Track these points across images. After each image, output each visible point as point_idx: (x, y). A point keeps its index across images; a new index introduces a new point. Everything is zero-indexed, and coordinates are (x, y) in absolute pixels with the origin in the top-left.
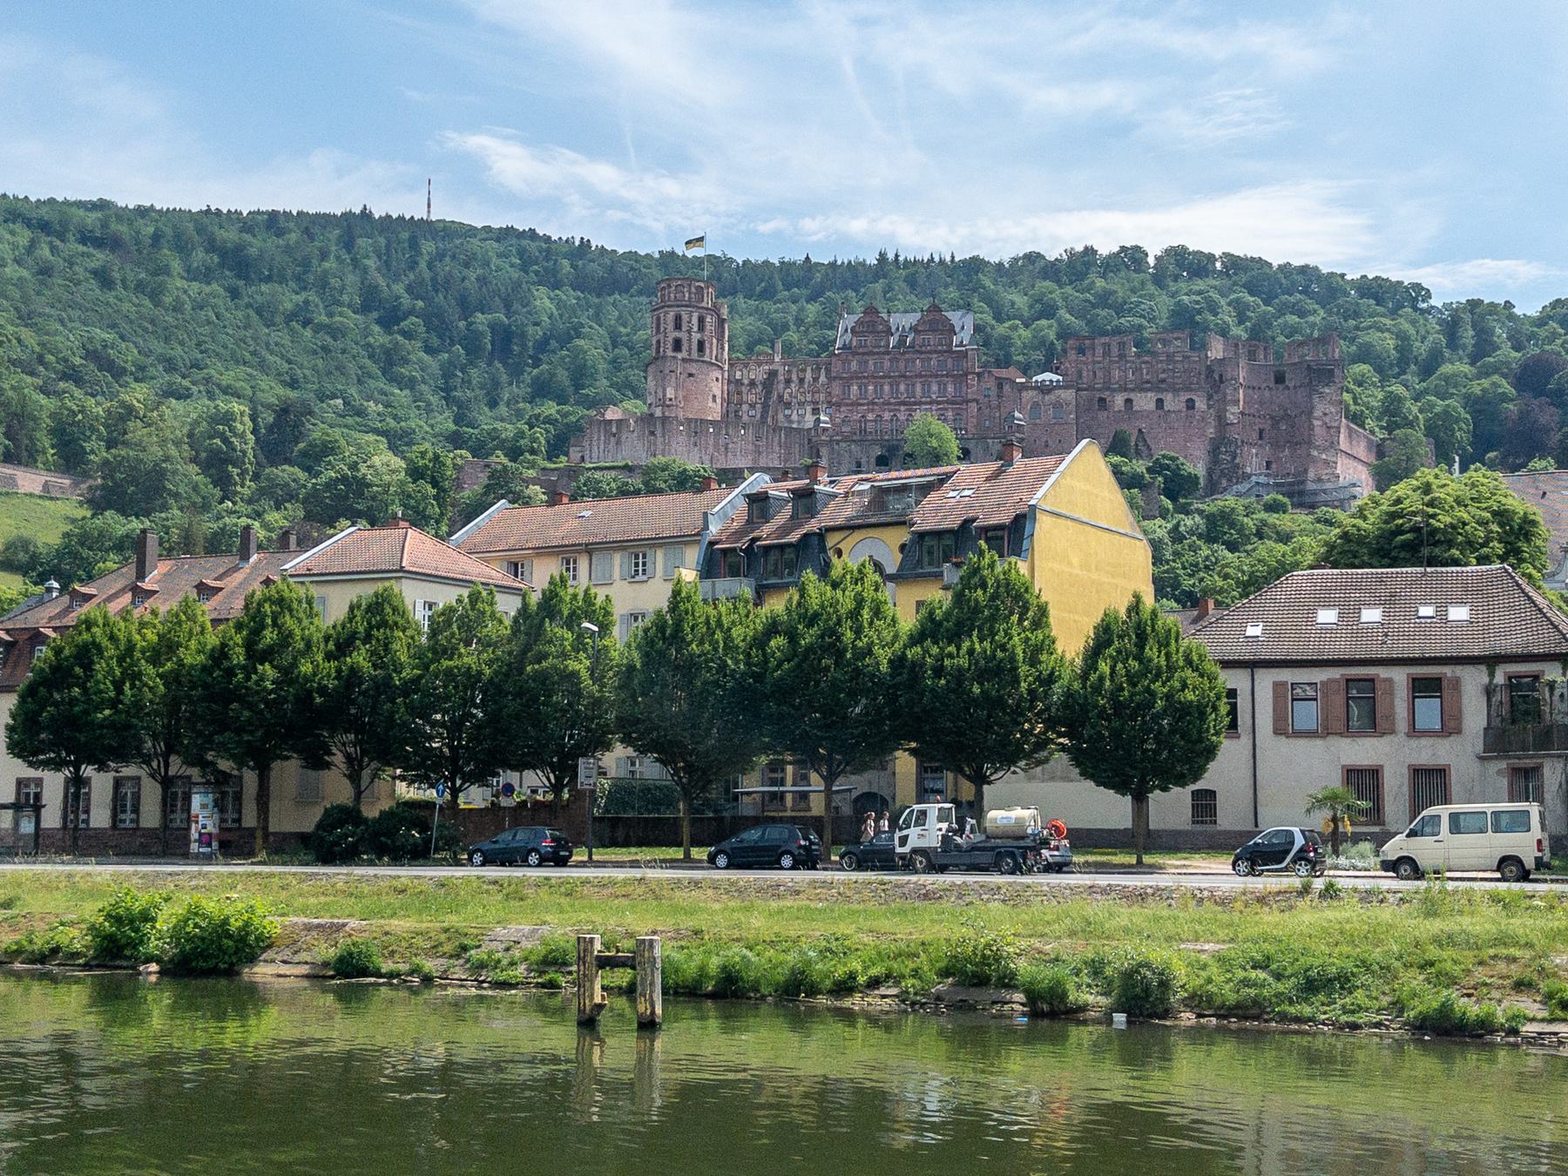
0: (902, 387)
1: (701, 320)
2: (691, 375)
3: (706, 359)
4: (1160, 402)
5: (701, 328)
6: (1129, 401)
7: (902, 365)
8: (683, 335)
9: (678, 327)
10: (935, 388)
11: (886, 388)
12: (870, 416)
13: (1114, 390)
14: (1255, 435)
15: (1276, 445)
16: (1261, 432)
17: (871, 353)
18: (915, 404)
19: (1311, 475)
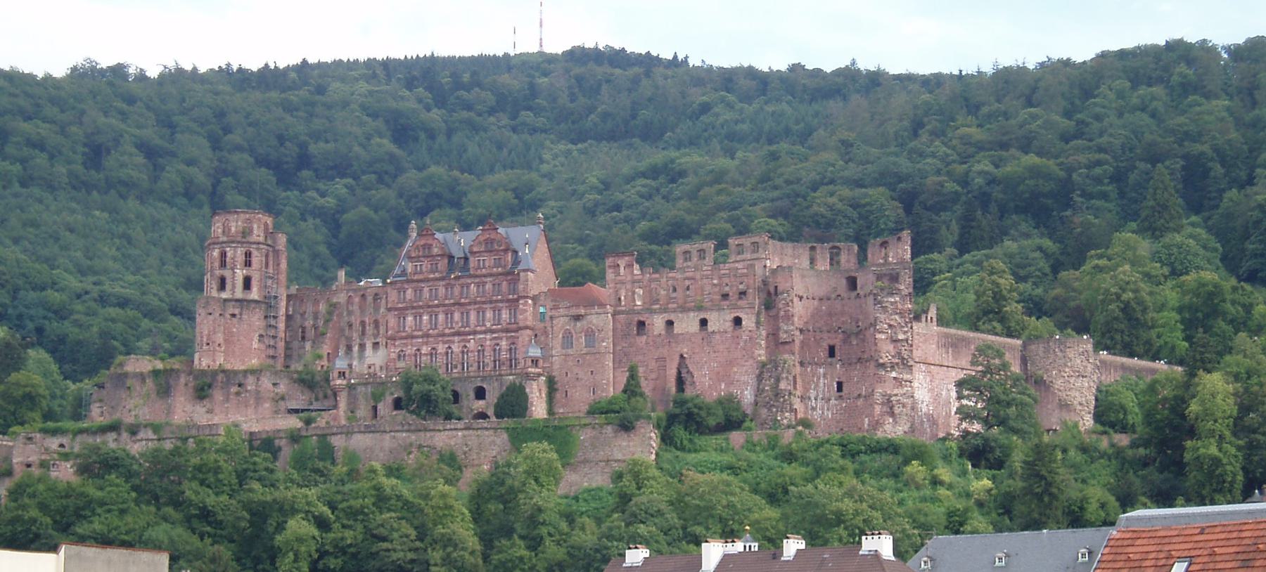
0: (457, 316)
1: (248, 255)
2: (233, 315)
3: (255, 294)
4: (704, 322)
5: (248, 263)
6: (670, 323)
7: (457, 290)
8: (227, 273)
9: (223, 264)
10: (489, 314)
11: (441, 317)
12: (425, 350)
13: (652, 312)
14: (823, 354)
15: (847, 364)
16: (832, 352)
17: (428, 280)
19: (878, 397)
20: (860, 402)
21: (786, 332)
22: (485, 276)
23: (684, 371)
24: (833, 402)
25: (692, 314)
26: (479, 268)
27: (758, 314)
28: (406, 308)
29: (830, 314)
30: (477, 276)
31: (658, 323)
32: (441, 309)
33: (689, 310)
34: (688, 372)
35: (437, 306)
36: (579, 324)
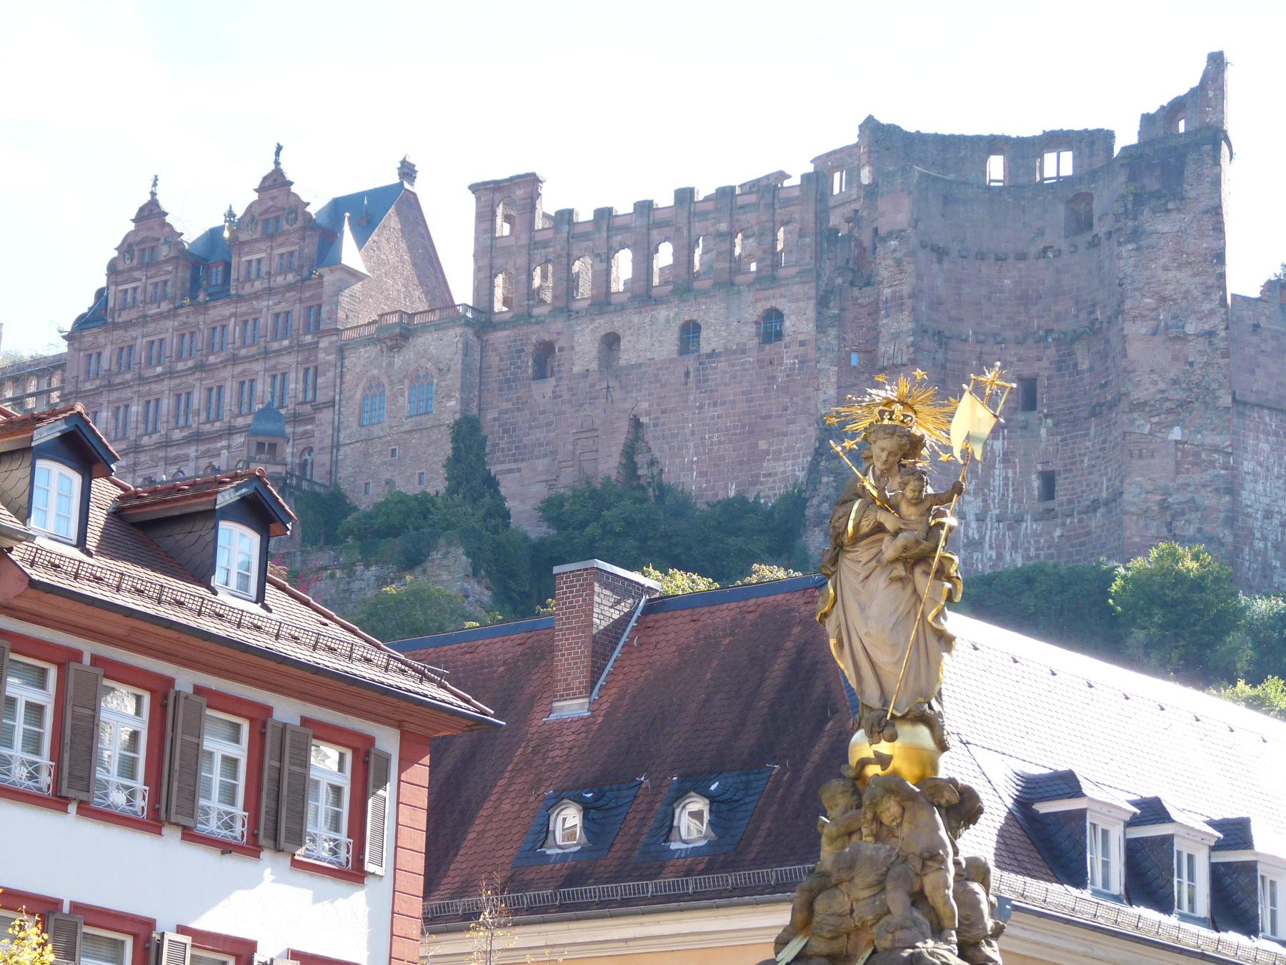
6: (611, 341)
18: (219, 436)
20: (1096, 521)
21: (896, 336)
22: (256, 296)
23: (641, 459)
24: (1029, 526)
25: (662, 313)
26: (248, 278)
27: (822, 302)
28: (97, 392)
29: (1024, 299)
30: (240, 298)
31: (583, 345)
32: (166, 385)
33: (659, 301)
34: (652, 463)
35: (159, 378)
36: (398, 361)
